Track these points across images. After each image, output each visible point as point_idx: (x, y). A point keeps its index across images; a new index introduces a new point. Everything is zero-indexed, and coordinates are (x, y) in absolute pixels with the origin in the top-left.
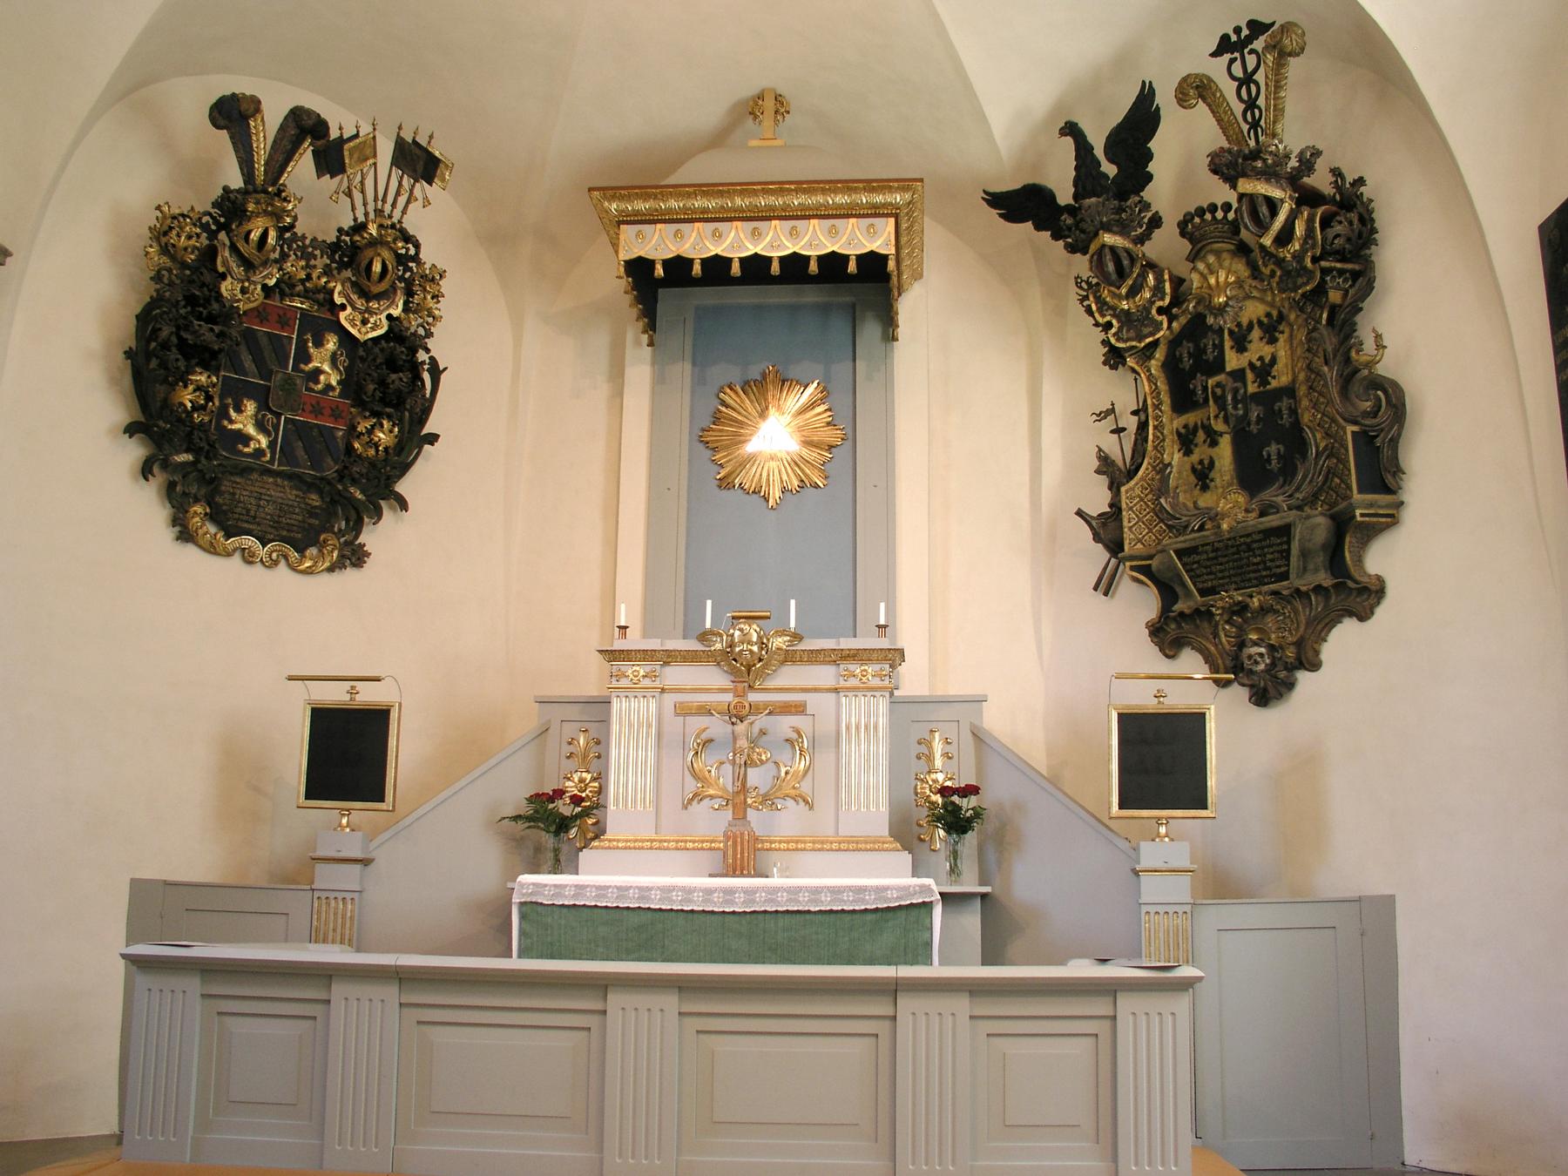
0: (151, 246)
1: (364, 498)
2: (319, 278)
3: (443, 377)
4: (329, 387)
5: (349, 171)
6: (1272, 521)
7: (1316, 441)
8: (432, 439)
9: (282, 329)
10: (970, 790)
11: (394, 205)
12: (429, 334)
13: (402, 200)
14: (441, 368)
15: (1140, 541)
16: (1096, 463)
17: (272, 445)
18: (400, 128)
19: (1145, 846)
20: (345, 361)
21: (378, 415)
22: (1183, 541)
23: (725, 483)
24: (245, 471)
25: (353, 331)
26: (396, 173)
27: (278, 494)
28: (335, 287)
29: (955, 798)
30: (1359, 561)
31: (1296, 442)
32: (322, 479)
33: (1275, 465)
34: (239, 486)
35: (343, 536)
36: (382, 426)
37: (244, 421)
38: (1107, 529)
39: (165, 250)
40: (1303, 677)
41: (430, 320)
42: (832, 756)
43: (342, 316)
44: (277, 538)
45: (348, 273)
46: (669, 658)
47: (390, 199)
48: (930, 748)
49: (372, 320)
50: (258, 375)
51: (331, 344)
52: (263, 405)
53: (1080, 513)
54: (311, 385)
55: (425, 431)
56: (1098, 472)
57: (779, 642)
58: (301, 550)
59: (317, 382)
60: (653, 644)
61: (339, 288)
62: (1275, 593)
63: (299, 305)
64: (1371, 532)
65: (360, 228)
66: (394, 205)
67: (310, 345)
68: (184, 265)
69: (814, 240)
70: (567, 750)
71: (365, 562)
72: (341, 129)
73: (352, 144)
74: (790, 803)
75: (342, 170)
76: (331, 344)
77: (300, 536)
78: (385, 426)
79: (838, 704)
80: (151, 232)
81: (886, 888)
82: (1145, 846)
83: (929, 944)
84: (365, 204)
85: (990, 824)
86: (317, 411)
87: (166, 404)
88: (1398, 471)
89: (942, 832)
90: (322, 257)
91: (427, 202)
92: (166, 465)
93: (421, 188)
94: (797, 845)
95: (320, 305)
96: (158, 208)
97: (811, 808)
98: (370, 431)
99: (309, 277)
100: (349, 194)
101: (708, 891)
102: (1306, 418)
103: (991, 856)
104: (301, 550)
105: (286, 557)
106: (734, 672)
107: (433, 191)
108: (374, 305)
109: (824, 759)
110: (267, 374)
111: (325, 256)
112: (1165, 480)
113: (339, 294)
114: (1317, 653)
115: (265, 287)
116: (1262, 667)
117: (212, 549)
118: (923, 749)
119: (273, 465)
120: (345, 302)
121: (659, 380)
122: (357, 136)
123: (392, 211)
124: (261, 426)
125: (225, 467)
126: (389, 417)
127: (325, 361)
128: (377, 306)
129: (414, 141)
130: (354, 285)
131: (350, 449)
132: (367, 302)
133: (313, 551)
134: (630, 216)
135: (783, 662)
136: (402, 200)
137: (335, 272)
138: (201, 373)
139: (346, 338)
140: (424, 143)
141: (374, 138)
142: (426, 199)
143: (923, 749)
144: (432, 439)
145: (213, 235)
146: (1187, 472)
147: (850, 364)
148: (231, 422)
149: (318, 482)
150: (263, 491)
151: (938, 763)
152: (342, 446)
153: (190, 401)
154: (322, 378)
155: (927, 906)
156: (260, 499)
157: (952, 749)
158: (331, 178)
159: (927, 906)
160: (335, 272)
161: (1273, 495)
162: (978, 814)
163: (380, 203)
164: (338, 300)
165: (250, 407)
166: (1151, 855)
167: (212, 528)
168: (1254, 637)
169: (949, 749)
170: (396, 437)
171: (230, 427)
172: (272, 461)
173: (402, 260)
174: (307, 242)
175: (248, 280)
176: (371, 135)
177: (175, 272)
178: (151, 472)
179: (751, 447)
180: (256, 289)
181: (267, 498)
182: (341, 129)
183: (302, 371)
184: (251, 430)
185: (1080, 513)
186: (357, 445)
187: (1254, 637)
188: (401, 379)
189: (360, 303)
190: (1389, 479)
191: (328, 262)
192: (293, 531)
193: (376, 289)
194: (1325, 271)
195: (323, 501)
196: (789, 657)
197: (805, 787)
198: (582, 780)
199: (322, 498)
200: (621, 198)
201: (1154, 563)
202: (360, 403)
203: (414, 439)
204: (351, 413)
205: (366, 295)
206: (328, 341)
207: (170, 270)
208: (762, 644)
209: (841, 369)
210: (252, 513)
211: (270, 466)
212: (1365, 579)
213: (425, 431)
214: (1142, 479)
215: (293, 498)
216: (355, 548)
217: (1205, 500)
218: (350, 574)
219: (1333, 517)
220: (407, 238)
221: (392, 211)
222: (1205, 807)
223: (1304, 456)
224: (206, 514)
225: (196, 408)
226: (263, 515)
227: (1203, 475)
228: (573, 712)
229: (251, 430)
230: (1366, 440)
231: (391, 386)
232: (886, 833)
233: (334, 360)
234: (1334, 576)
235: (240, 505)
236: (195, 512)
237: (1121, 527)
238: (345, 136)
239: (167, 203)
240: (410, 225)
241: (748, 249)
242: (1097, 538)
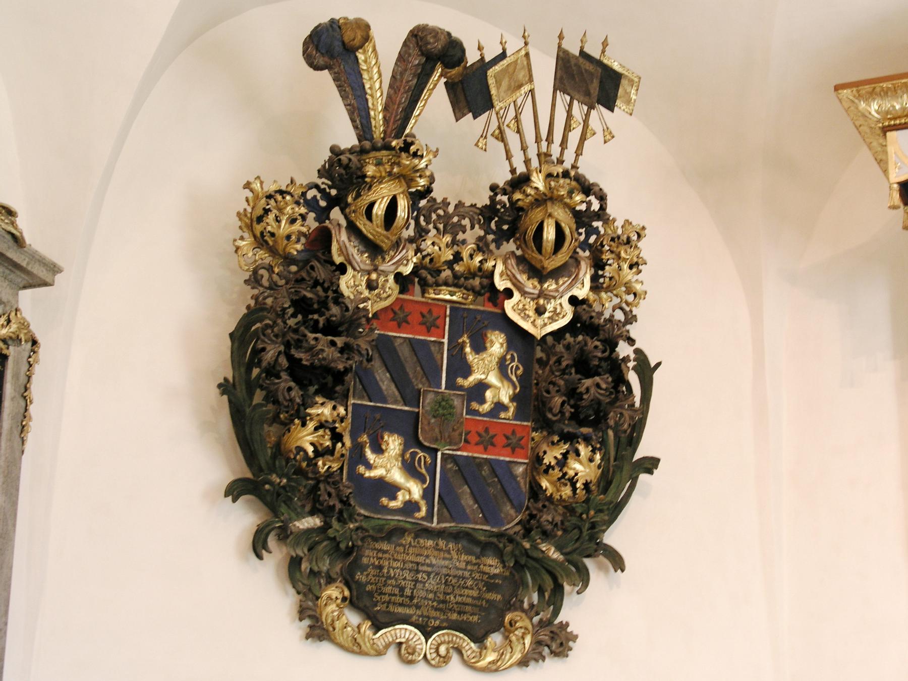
0: (242, 238)
1: (561, 558)
2: (471, 256)
3: (656, 376)
4: (499, 407)
5: (498, 105)
8: (650, 465)
9: (429, 332)
12: (631, 319)
13: (574, 137)
14: (652, 365)
17: (428, 494)
18: (561, 37)
20: (517, 368)
24: (393, 533)
25: (526, 325)
26: (562, 100)
27: (443, 563)
28: (494, 266)
32: (500, 535)
34: (386, 556)
35: (537, 614)
36: (578, 454)
39: (261, 241)
41: (630, 298)
43: (509, 305)
44: (445, 624)
45: (510, 246)
49: (550, 307)
50: (399, 398)
51: (497, 344)
52: (412, 440)
54: (475, 405)
55: (638, 455)
58: (479, 639)
59: (482, 401)
61: (500, 268)
63: (448, 297)
65: (520, 182)
67: (468, 349)
68: (288, 260)
71: (570, 649)
72: (480, 48)
73: (497, 68)
75: (488, 104)
76: (497, 344)
77: (476, 618)
78: (582, 453)
80: (240, 219)
84: (524, 149)
86: (488, 443)
87: (279, 450)
90: (472, 227)
91: (609, 136)
92: (284, 535)
93: (599, 116)
95: (477, 294)
96: (247, 186)
98: (562, 462)
99: (457, 257)
100: (501, 137)
104: (479, 639)
105: (459, 651)
107: (615, 118)
108: (550, 285)
110: (413, 397)
111: (477, 226)
113: (501, 275)
115: (398, 277)
117: (355, 648)
119: (432, 522)
120: (509, 285)
122: (503, 56)
123: (562, 153)
124: (410, 469)
125: (367, 531)
126: (587, 440)
128: (554, 286)
129: (582, 53)
130: (521, 260)
131: (535, 491)
132: (541, 282)
133: (495, 639)
134: (900, 117)
136: (574, 137)
137: (493, 246)
138: (322, 404)
139: (517, 335)
140: (596, 54)
141: (527, 55)
144: (650, 465)
145: (323, 214)
148: (369, 467)
149: (494, 540)
150: (420, 559)
152: (524, 487)
153: (312, 444)
154: (489, 394)
156: (418, 572)
158: (475, 117)
160: (493, 246)
163: (544, 144)
164: (501, 284)
165: (394, 444)
167: (353, 618)
170: (599, 467)
171: (367, 474)
172: (429, 516)
173: (582, 219)
174: (451, 209)
175: (376, 270)
176: (523, 52)
177: (276, 270)
178: (265, 546)
180: (387, 281)
181: (425, 568)
182: (480, 48)
183: (461, 388)
184: (397, 476)
186: (545, 484)
188: (598, 386)
189: (531, 285)
191: (482, 233)
192: (465, 613)
193: (551, 264)
195: (504, 567)
199: (503, 562)
200: (885, 93)
202: (544, 424)
204: (533, 439)
205: (538, 273)
206: (492, 342)
207: (270, 269)
210: (408, 592)
211: (429, 525)
213: (638, 455)
215: (463, 565)
216: (554, 629)
220: (587, 189)
221: (562, 153)
224: (344, 599)
225: (319, 453)
226: (423, 594)
229: (397, 476)
231: (585, 397)
233: (502, 367)
235: (389, 582)
236: (330, 598)
238: (488, 59)
239: (258, 178)
240: (589, 170)
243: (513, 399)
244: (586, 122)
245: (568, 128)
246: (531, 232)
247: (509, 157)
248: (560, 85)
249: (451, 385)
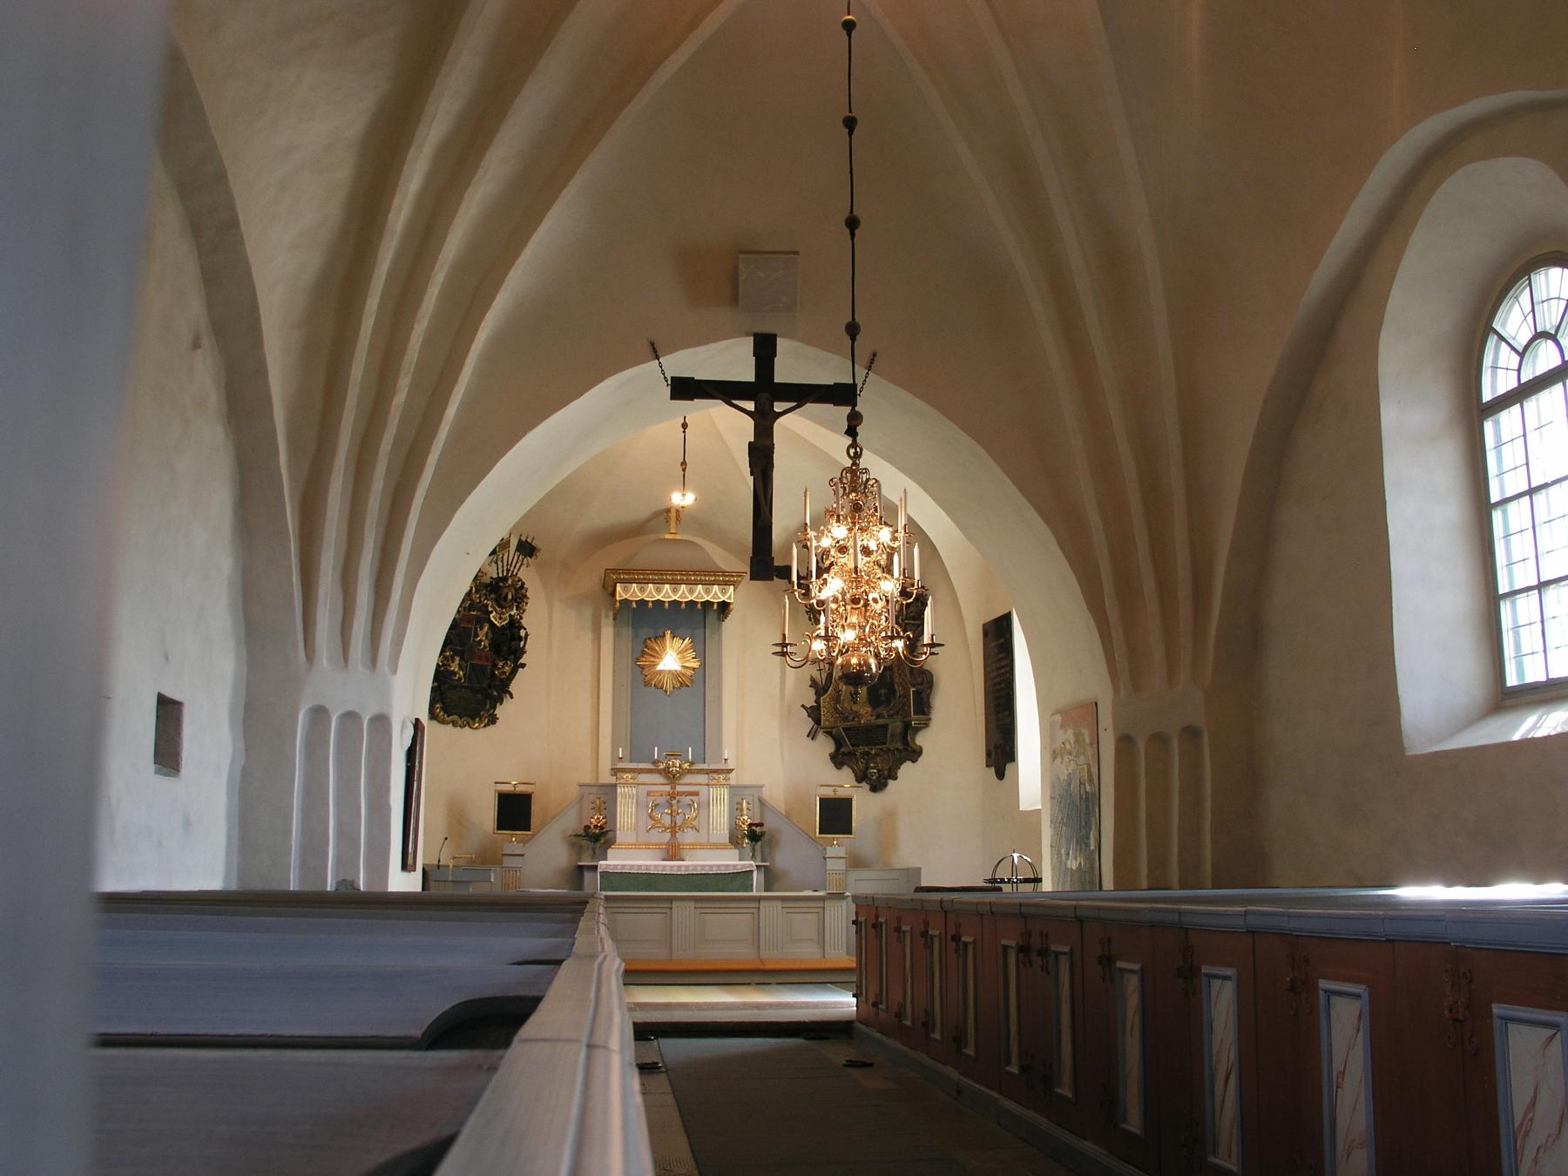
6: (880, 721)
7: (899, 690)
10: (761, 825)
11: (515, 567)
12: (521, 618)
15: (828, 720)
16: (810, 683)
17: (464, 675)
19: (828, 848)
21: (506, 659)
23: (647, 684)
25: (496, 623)
29: (754, 828)
30: (913, 739)
31: (892, 691)
33: (883, 698)
38: (814, 712)
40: (891, 782)
42: (706, 812)
43: (491, 615)
45: (493, 596)
46: (641, 771)
47: (513, 565)
48: (742, 806)
52: (462, 659)
53: (803, 706)
56: (810, 686)
57: (686, 766)
58: (474, 719)
60: (634, 766)
62: (881, 749)
64: (917, 730)
65: (505, 579)
66: (515, 567)
69: (700, 594)
70: (592, 806)
74: (689, 830)
79: (709, 791)
81: (737, 865)
82: (828, 848)
83: (752, 885)
84: (503, 567)
85: (765, 838)
86: (480, 659)
88: (929, 707)
89: (747, 841)
94: (694, 846)
97: (698, 831)
98: (503, 667)
99: (480, 601)
100: (497, 563)
101: (656, 866)
102: (896, 680)
103: (767, 850)
106: (668, 778)
109: (703, 812)
112: (839, 696)
114: (896, 773)
116: (875, 777)
118: (739, 806)
121: (617, 635)
127: (483, 634)
131: (493, 675)
135: (686, 774)
142: (528, 563)
143: (739, 806)
146: (848, 694)
147: (703, 629)
151: (745, 812)
152: (489, 671)
155: (752, 871)
157: (749, 806)
159: (752, 871)
161: (883, 710)
162: (762, 834)
164: (490, 609)
166: (830, 852)
168: (872, 765)
169: (749, 806)
179: (659, 668)
185: (803, 706)
187: (872, 765)
190: (926, 709)
194: (906, 624)
196: (690, 772)
197: (695, 823)
198: (598, 818)
201: (834, 731)
205: (501, 607)
208: (680, 767)
209: (699, 632)
212: (915, 747)
214: (830, 694)
217: (855, 708)
218: (491, 727)
219: (904, 722)
220: (520, 580)
222: (851, 834)
223: (894, 696)
228: (594, 790)
230: (917, 694)
232: (728, 841)
234: (904, 745)
237: (820, 714)
241: (671, 597)
242: (809, 716)
243: (490, 644)
244: (523, 560)
245: (517, 563)
246: (504, 595)
247: (498, 569)
248: (517, 550)
249: (474, 641)
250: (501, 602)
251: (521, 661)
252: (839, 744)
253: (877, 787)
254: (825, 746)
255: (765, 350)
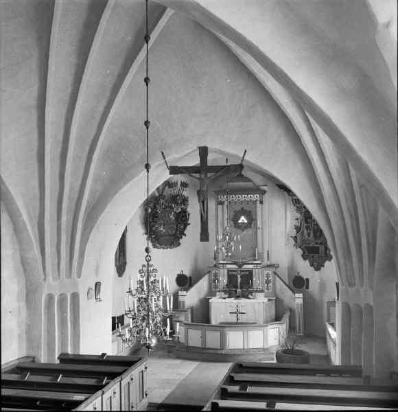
22: (306, 245)
37: (162, 229)
40: (322, 268)
107: (187, 189)
124: (164, 228)
203: (186, 225)
227: (309, 234)
229: (162, 229)
250: (177, 203)
251: (189, 222)
252: (304, 253)
253: (317, 269)
254: (300, 251)
255: (204, 152)
